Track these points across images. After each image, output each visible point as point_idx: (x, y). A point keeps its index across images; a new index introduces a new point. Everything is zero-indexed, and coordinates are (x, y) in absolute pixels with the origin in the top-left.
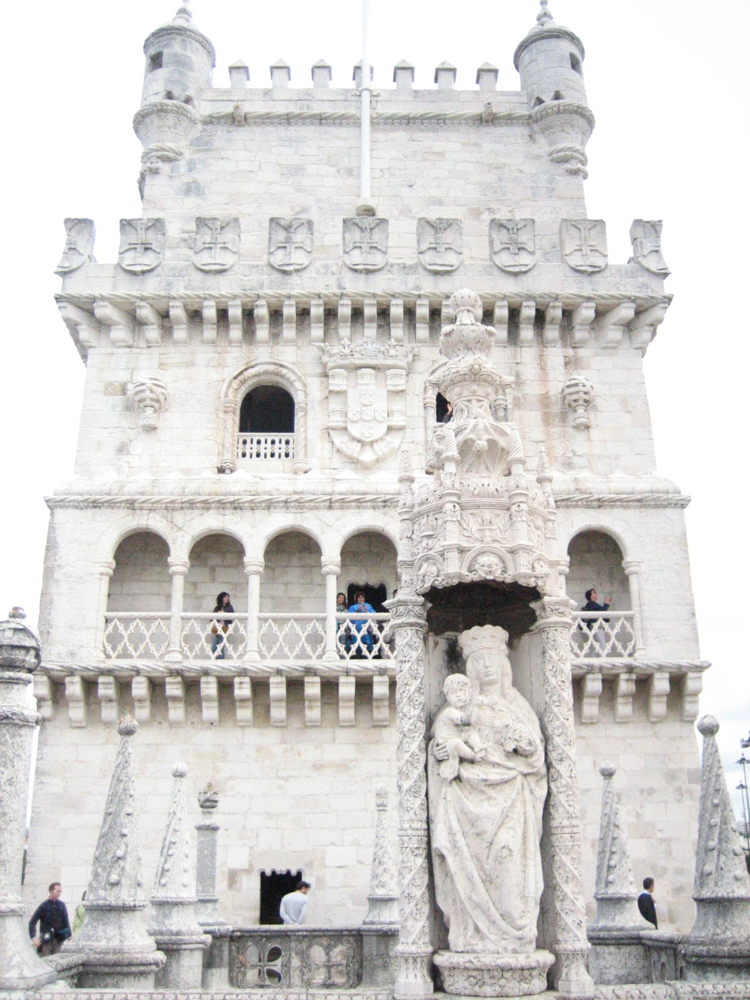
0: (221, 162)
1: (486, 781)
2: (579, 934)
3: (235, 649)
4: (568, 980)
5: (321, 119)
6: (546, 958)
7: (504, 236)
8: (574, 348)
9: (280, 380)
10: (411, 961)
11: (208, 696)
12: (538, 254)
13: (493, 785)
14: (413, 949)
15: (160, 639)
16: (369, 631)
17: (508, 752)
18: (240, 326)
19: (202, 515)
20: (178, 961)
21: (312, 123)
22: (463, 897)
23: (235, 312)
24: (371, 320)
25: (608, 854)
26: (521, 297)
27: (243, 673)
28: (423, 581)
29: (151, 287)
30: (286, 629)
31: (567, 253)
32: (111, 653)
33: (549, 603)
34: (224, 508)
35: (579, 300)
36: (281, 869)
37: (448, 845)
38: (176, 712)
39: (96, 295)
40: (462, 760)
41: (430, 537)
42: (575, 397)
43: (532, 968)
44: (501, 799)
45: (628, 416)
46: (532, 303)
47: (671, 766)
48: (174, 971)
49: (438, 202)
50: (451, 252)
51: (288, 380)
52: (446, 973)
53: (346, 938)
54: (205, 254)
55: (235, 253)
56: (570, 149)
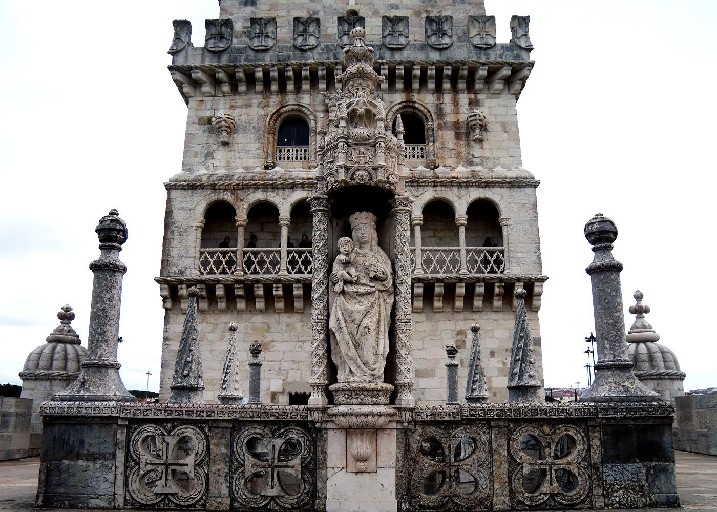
1: (357, 292)
2: (408, 375)
3: (274, 269)
4: (400, 399)
6: (389, 386)
8: (474, 94)
9: (302, 114)
10: (316, 388)
12: (455, 38)
13: (362, 295)
14: (317, 381)
17: (371, 278)
18: (277, 83)
19: (254, 192)
22: (344, 354)
23: (274, 74)
26: (443, 62)
27: (278, 281)
28: (327, 187)
29: (225, 60)
31: (471, 36)
32: (204, 271)
33: (398, 199)
34: (267, 188)
35: (479, 65)
36: (300, 391)
37: (336, 327)
39: (192, 65)
40: (346, 282)
41: (331, 162)
42: (474, 123)
43: (378, 390)
44: (366, 302)
45: (506, 134)
46: (450, 67)
49: (396, 7)
50: (402, 37)
51: (305, 114)
52: (334, 394)
54: (256, 40)
55: (274, 39)
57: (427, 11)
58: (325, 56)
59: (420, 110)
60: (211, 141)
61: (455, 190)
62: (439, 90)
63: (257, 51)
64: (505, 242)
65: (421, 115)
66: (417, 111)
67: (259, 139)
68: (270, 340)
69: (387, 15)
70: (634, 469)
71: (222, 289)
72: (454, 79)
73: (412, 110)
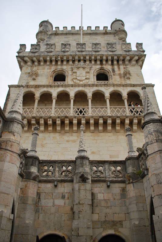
0: (53, 41)
5: (73, 34)
7: (110, 46)
9: (62, 72)
11: (41, 123)
16: (81, 110)
20: (13, 124)
21: (71, 35)
23: (54, 58)
24: (82, 60)
25: (147, 104)
27: (50, 117)
39: (25, 55)
45: (138, 77)
48: (11, 127)
53: (72, 163)
56: (122, 37)
59: (106, 71)
60: (29, 79)
61: (122, 87)
62: (112, 64)
65: (106, 72)
66: (105, 71)
67: (47, 78)
68: (45, 143)
69: (94, 43)
71: (26, 121)
72: (118, 61)
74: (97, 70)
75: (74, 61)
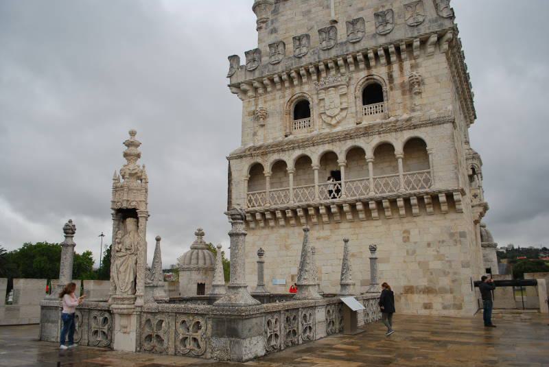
6: (133, 296)
8: (415, 59)
15: (264, 200)
23: (285, 77)
27: (288, 208)
29: (257, 74)
30: (309, 190)
38: (272, 223)
45: (439, 85)
47: (452, 231)
49: (362, 9)
54: (273, 57)
57: (383, 6)
58: (313, 58)
61: (394, 134)
63: (274, 64)
64: (431, 166)
69: (348, 20)
70: (224, 341)
73: (372, 81)
74: (361, 83)
75: (318, 72)
